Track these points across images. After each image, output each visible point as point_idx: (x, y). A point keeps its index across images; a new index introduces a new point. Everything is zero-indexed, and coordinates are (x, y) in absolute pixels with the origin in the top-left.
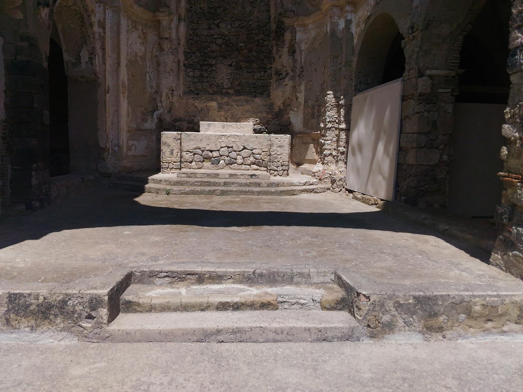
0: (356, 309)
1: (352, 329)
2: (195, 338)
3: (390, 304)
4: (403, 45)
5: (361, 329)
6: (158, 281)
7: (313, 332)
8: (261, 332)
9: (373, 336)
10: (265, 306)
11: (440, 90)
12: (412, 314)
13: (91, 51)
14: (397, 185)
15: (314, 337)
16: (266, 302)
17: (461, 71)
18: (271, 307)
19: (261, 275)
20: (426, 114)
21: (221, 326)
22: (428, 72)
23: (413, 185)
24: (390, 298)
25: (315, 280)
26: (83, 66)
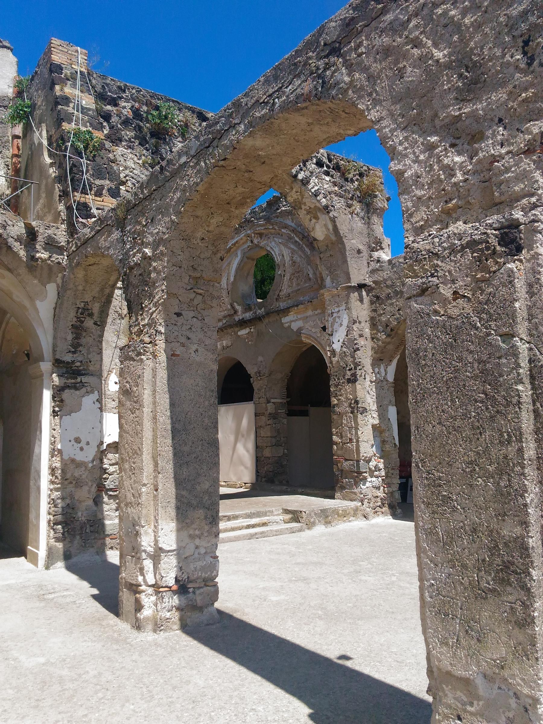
0: (300, 519)
1: (302, 526)
3: (313, 514)
4: (252, 382)
5: (305, 526)
9: (308, 529)
10: (264, 524)
11: (279, 411)
12: (321, 517)
14: (257, 472)
17: (289, 399)
19: (254, 514)
20: (274, 425)
21: (256, 532)
22: (273, 400)
23: (271, 470)
24: (313, 511)
25: (275, 513)
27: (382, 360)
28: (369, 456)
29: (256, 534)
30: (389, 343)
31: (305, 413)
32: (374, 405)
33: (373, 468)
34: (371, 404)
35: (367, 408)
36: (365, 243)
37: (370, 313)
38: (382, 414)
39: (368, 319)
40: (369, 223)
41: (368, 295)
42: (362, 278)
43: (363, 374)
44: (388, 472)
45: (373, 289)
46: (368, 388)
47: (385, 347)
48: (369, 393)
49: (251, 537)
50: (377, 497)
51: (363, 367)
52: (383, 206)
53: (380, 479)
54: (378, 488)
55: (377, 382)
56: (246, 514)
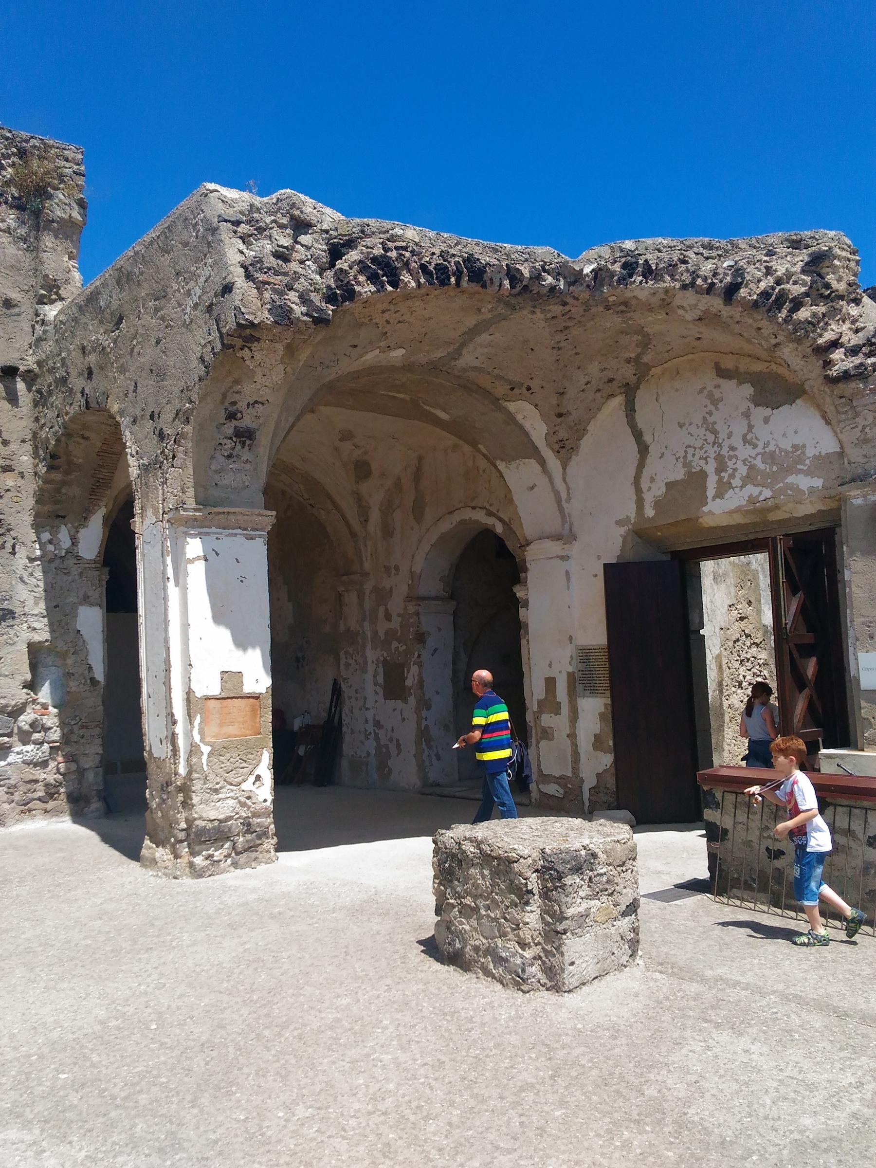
27: (64, 517)
28: (13, 703)
30: (64, 483)
32: (36, 604)
33: (27, 727)
34: (30, 602)
35: (18, 611)
36: (26, 288)
37: (33, 425)
38: (60, 621)
39: (30, 436)
40: (36, 249)
41: (29, 390)
42: (17, 355)
43: (9, 545)
44: (72, 732)
45: (36, 376)
46: (20, 572)
47: (58, 491)
48: (23, 581)
50: (36, 781)
51: (9, 530)
52: (66, 216)
53: (46, 746)
54: (44, 764)
55: (47, 559)
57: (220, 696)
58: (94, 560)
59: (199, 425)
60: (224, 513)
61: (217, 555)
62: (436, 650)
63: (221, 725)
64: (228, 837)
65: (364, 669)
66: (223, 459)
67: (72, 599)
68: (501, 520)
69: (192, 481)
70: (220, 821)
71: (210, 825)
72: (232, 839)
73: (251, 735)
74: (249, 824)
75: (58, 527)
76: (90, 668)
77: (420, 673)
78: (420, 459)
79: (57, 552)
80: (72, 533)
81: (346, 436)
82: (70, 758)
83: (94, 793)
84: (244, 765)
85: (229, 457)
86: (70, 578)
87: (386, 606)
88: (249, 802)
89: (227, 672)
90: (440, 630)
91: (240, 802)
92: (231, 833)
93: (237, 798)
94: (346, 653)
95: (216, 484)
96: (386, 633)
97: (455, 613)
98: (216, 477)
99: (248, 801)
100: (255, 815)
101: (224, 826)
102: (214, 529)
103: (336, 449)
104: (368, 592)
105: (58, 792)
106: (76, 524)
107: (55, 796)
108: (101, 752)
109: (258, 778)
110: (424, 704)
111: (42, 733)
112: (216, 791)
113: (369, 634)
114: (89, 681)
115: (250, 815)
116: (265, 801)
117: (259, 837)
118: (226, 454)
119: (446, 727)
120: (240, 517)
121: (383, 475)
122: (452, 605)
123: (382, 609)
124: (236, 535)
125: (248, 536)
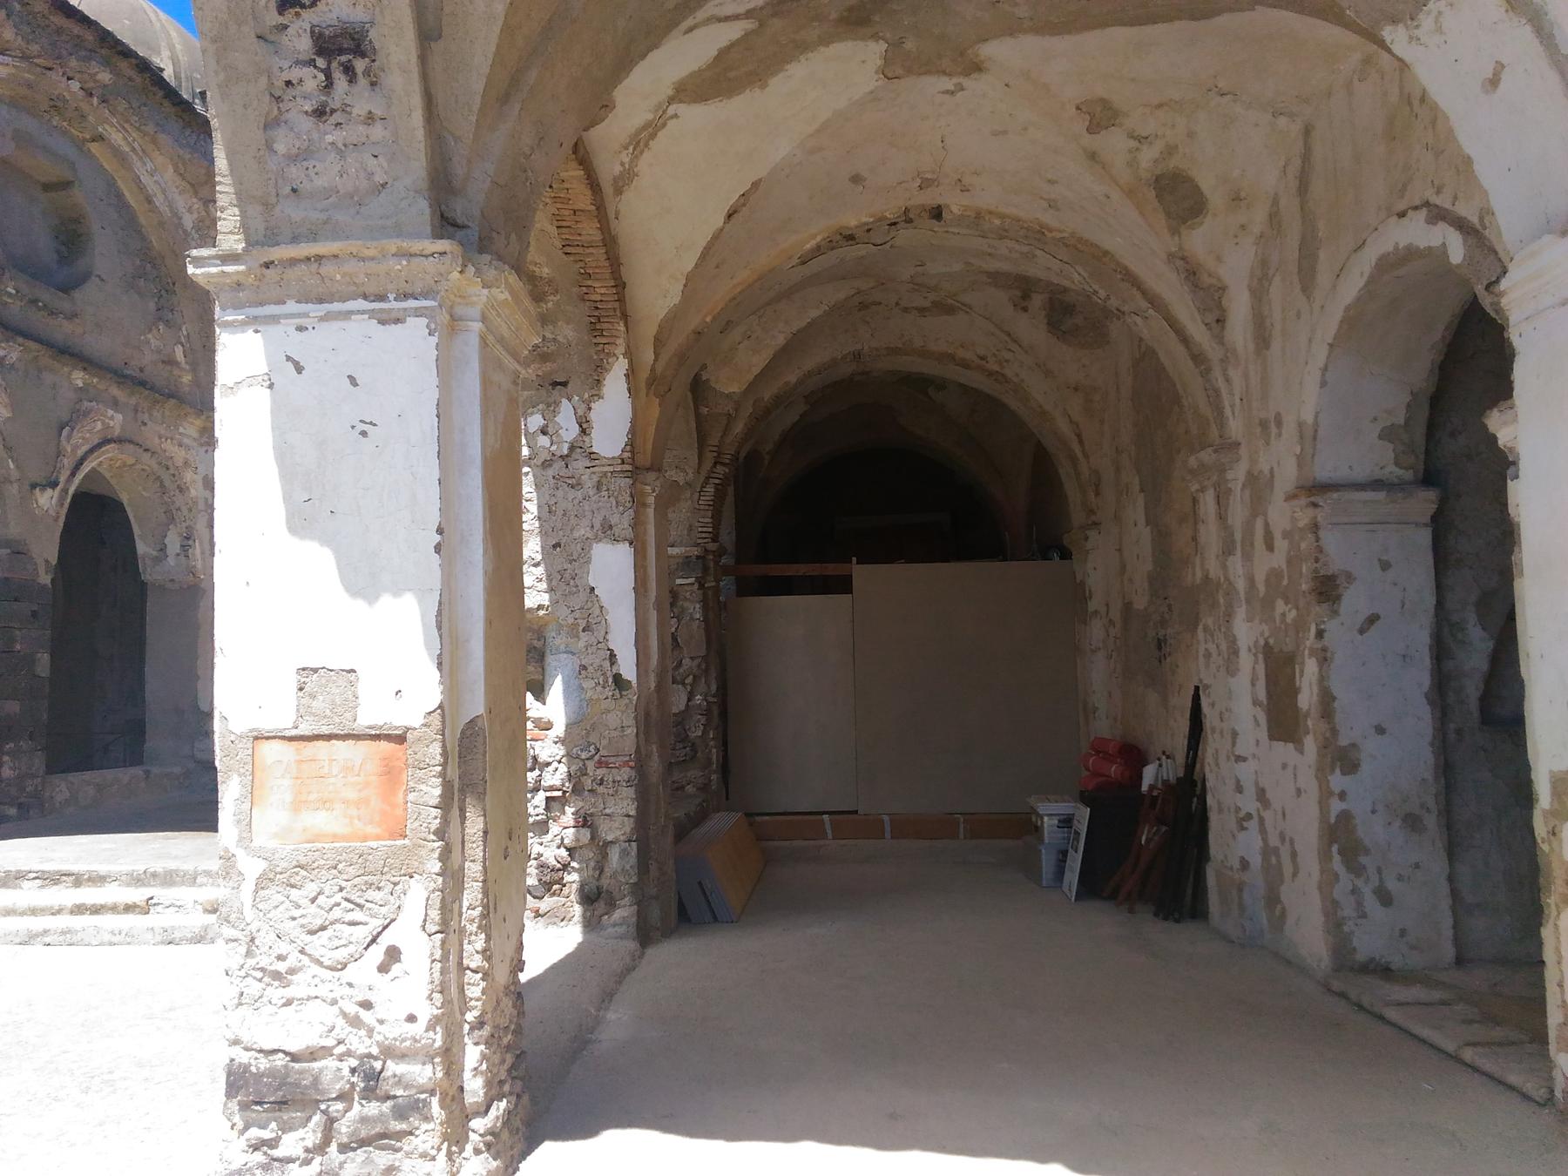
2: (18, 941)
6: (26, 884)
7: (157, 931)
8: (95, 932)
11: (679, 581)
13: (185, 535)
15: (159, 938)
16: (130, 903)
18: (137, 910)
19: (154, 875)
26: (171, 561)
27: (564, 384)
29: (46, 932)
31: (843, 585)
38: (562, 573)
49: (29, 939)
55: (538, 461)
56: (130, 874)
57: (294, 732)
58: (619, 457)
59: (214, 41)
60: (309, 259)
61: (299, 369)
62: (1372, 619)
63: (297, 806)
64: (318, 1101)
65: (1231, 669)
66: (307, 124)
67: (582, 531)
68: (1461, 225)
69: (232, 190)
70: (295, 1058)
71: (264, 1063)
72: (323, 1107)
73: (378, 838)
74: (373, 1077)
75: (557, 404)
76: (612, 657)
77: (1322, 679)
78: (1307, 131)
79: (554, 448)
80: (580, 412)
81: (1100, 116)
82: (584, 821)
83: (626, 889)
84: (357, 915)
85: (320, 113)
86: (579, 494)
87: (1265, 515)
88: (365, 1015)
89: (315, 670)
90: (1385, 566)
91: (344, 1015)
92: (322, 1092)
93: (334, 1002)
94: (1206, 629)
95: (294, 191)
96: (1267, 581)
97: (1440, 525)
98: (294, 172)
99: (364, 1014)
100: (388, 1052)
101: (301, 1072)
102: (292, 306)
103: (1093, 156)
104: (1237, 487)
105: (560, 881)
106: (586, 396)
107: (555, 887)
108: (632, 813)
109: (393, 954)
110: (1344, 759)
111: (537, 772)
112: (277, 975)
113: (1241, 585)
114: (610, 680)
115: (375, 1051)
116: (412, 1019)
117: (401, 1113)
118: (308, 108)
119: (1412, 822)
120: (351, 266)
121: (1237, 198)
122: (1424, 502)
123: (1259, 525)
124: (347, 315)
125: (385, 316)
